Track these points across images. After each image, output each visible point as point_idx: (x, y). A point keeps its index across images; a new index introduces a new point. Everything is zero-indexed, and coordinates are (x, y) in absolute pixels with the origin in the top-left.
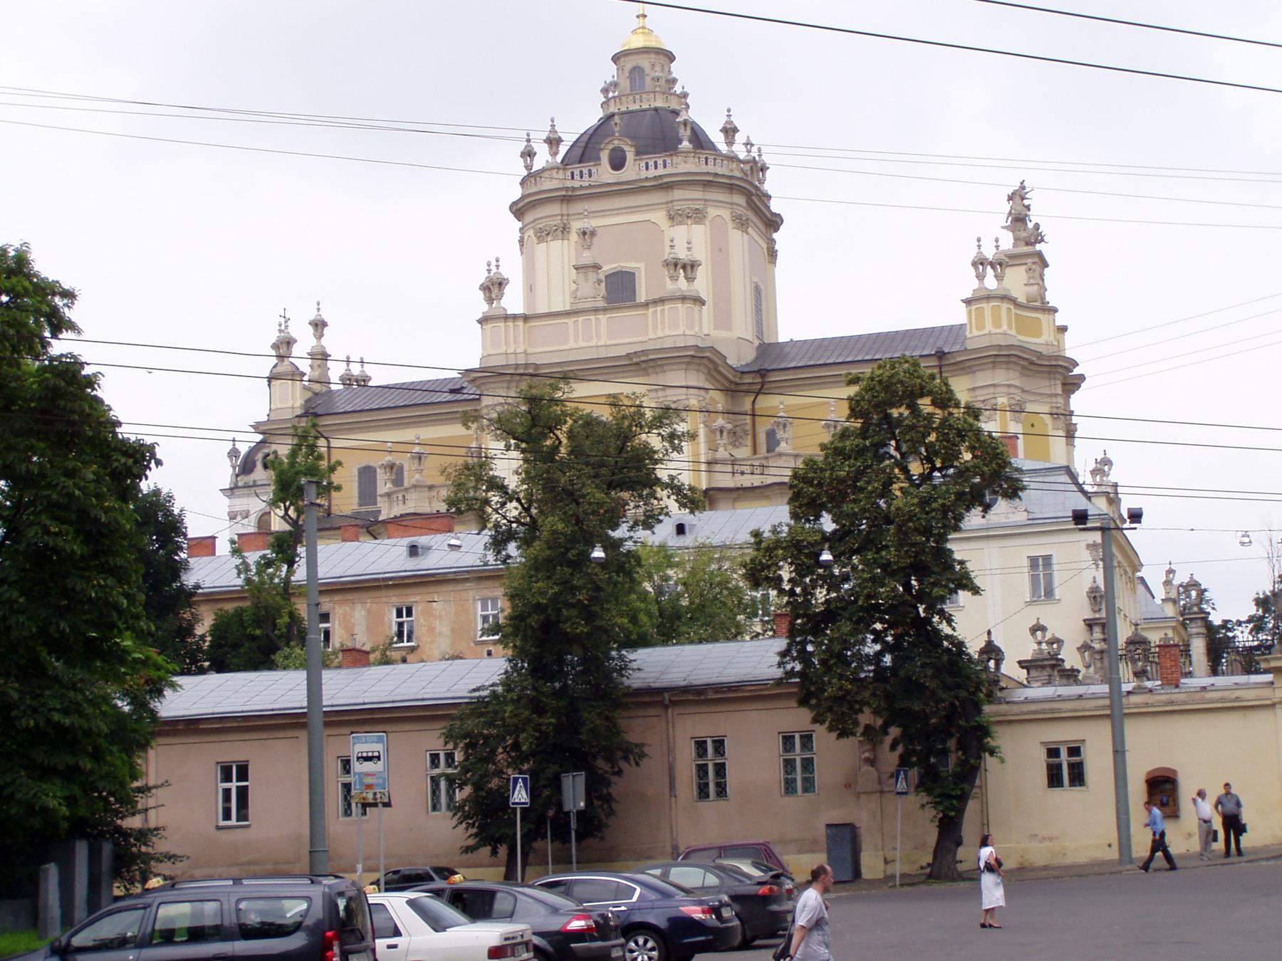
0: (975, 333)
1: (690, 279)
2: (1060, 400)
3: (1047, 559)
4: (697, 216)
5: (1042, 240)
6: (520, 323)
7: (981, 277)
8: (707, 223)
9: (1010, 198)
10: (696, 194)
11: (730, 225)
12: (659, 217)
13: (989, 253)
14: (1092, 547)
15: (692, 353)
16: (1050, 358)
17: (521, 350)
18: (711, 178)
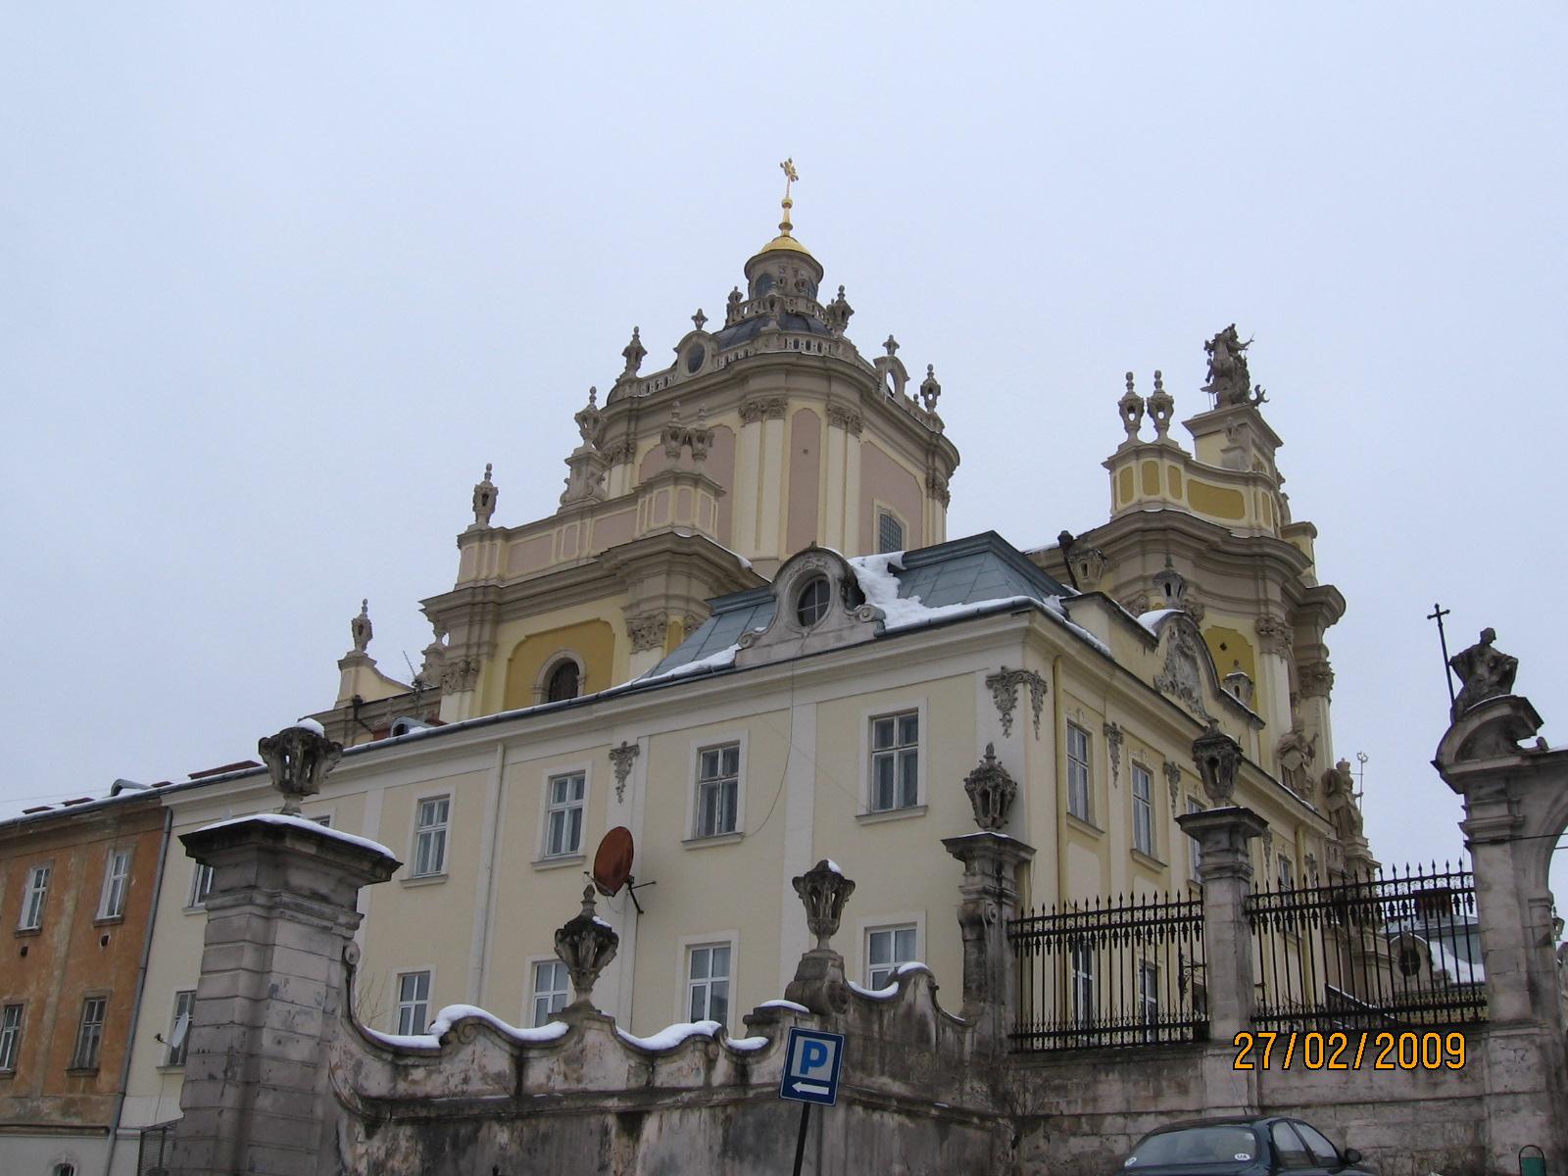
0: (1121, 506)
1: (697, 456)
2: (1279, 614)
3: (910, 723)
4: (774, 408)
5: (1260, 399)
6: (499, 542)
7: (1132, 428)
8: (789, 418)
9: (1209, 347)
10: (778, 381)
11: (824, 421)
12: (731, 419)
13: (1145, 391)
14: (1003, 683)
15: (668, 545)
16: (1251, 541)
17: (495, 573)
18: (793, 360)
